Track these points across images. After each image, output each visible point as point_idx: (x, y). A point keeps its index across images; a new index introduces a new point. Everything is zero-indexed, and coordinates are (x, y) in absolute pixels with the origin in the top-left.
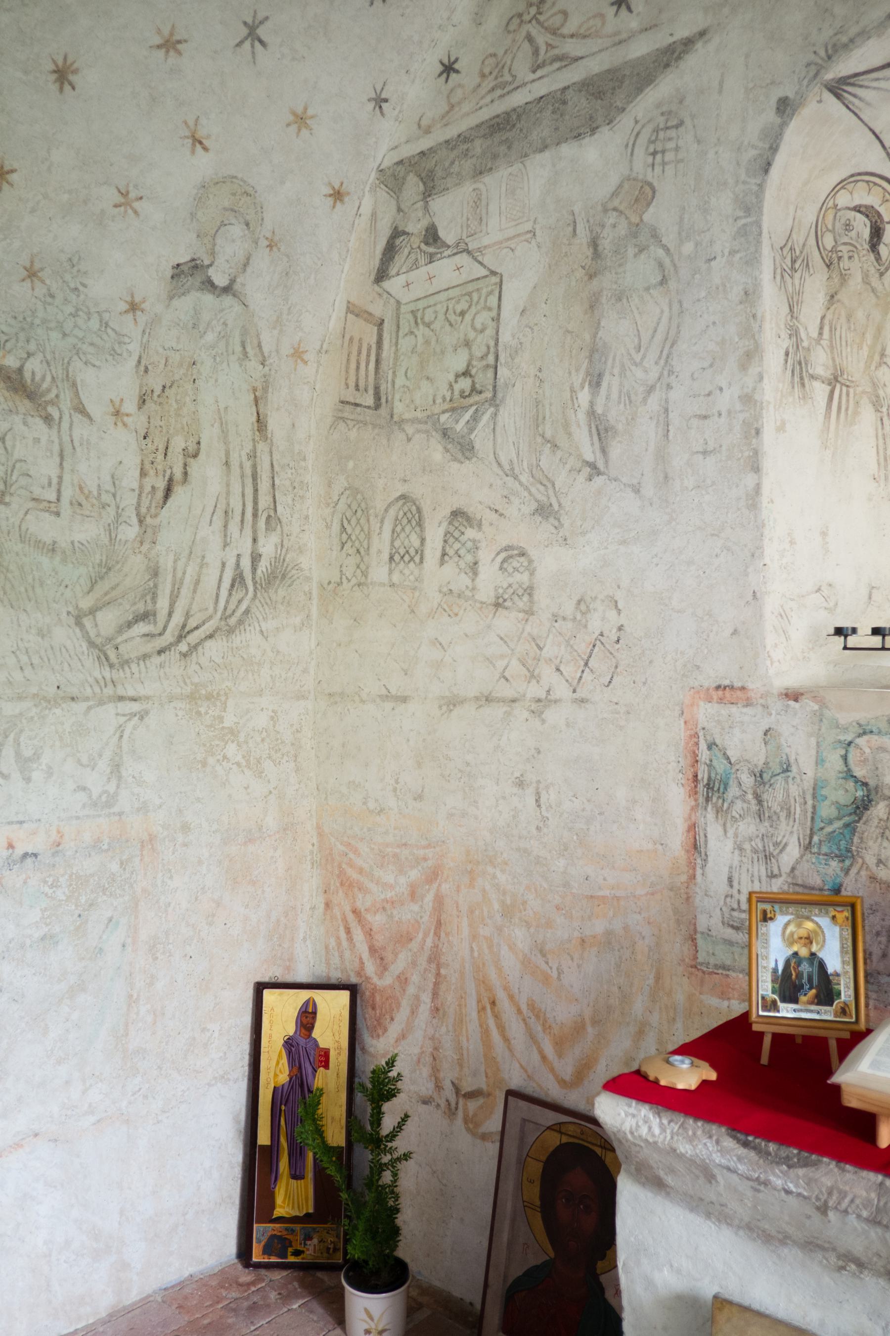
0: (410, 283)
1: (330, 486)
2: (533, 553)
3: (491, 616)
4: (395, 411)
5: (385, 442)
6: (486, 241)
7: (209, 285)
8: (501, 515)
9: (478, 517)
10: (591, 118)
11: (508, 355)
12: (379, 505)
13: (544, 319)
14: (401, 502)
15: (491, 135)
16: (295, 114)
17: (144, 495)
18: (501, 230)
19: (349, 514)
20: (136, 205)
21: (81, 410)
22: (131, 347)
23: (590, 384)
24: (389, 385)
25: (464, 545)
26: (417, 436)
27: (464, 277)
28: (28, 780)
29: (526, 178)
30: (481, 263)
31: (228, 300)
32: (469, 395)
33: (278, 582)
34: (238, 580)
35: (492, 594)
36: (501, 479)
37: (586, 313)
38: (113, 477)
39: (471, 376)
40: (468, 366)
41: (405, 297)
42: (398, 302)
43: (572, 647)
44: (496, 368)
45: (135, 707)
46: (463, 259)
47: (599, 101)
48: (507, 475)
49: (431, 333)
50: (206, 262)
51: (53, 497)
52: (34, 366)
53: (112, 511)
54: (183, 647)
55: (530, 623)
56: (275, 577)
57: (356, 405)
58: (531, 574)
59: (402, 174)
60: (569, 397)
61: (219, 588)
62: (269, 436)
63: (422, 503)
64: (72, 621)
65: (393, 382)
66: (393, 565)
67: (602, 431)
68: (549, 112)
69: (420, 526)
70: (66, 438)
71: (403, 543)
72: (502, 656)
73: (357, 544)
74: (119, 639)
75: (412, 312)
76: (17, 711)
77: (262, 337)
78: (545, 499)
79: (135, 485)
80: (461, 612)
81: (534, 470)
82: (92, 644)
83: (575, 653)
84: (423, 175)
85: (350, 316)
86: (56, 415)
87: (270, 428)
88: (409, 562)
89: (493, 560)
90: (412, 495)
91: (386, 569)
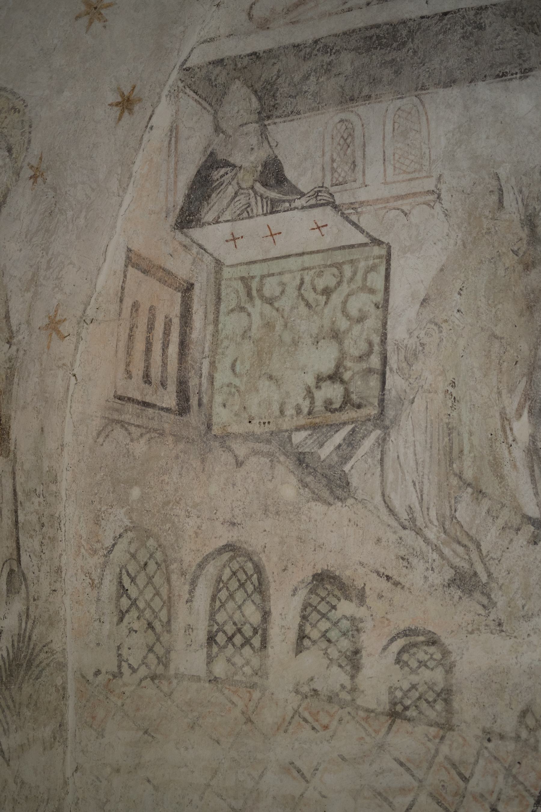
0: (235, 237)
1: (97, 523)
2: (447, 640)
3: (384, 730)
4: (215, 419)
5: (196, 464)
6: (363, 195)
8: (397, 584)
9: (359, 584)
10: (521, 55)
11: (402, 358)
12: (188, 555)
13: (458, 315)
14: (226, 556)
15: (368, 50)
18: (385, 183)
19: (132, 568)
23: (530, 412)
24: (204, 381)
25: (336, 624)
26: (253, 459)
27: (328, 242)
29: (424, 119)
30: (356, 225)
32: (341, 409)
33: (22, 673)
35: (385, 698)
36: (395, 532)
37: (521, 315)
39: (342, 381)
40: (338, 367)
41: (231, 256)
42: (218, 263)
43: (515, 777)
44: (384, 374)
46: (326, 215)
47: (532, 35)
48: (404, 528)
49: (274, 313)
55: (447, 742)
56: (19, 666)
57: (146, 404)
58: (447, 672)
59: (222, 79)
60: (499, 426)
62: (12, 448)
63: (264, 559)
65: (211, 379)
66: (215, 649)
68: (457, 37)
69: (261, 592)
71: (231, 618)
72: (403, 791)
73: (148, 614)
75: (242, 279)
77: (11, 304)
78: (467, 566)
80: (335, 723)
81: (447, 523)
83: (520, 787)
84: (258, 86)
85: (131, 271)
87: (13, 436)
88: (243, 646)
89: (385, 649)
90: (245, 546)
91: (202, 655)
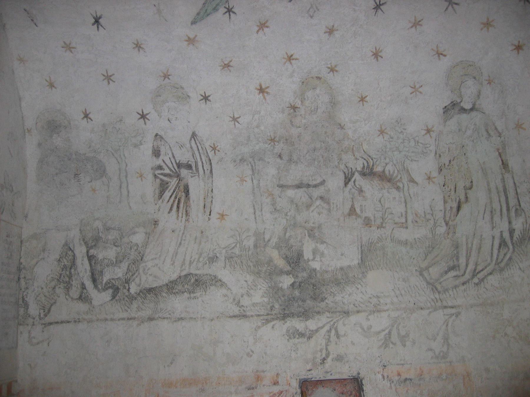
7: (463, 110)
16: (483, 23)
17: (447, 212)
20: (420, 90)
21: (412, 181)
22: (431, 148)
28: (404, 346)
31: (474, 114)
33: (526, 242)
34: (503, 243)
38: (430, 206)
45: (453, 311)
50: (459, 101)
51: (403, 220)
52: (389, 168)
53: (432, 222)
54: (476, 280)
61: (492, 249)
62: (511, 169)
64: (418, 273)
70: (407, 194)
74: (442, 280)
76: (397, 315)
77: (496, 125)
79: (442, 208)
82: (428, 283)
86: (401, 185)
87: (510, 165)
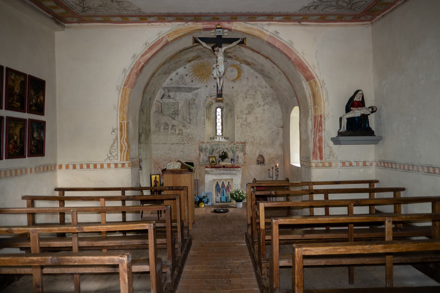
0: (165, 100)
67: (190, 120)
